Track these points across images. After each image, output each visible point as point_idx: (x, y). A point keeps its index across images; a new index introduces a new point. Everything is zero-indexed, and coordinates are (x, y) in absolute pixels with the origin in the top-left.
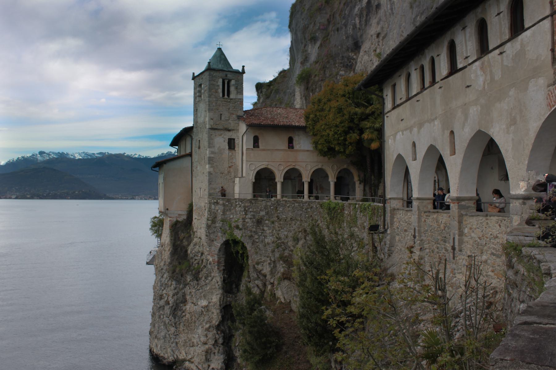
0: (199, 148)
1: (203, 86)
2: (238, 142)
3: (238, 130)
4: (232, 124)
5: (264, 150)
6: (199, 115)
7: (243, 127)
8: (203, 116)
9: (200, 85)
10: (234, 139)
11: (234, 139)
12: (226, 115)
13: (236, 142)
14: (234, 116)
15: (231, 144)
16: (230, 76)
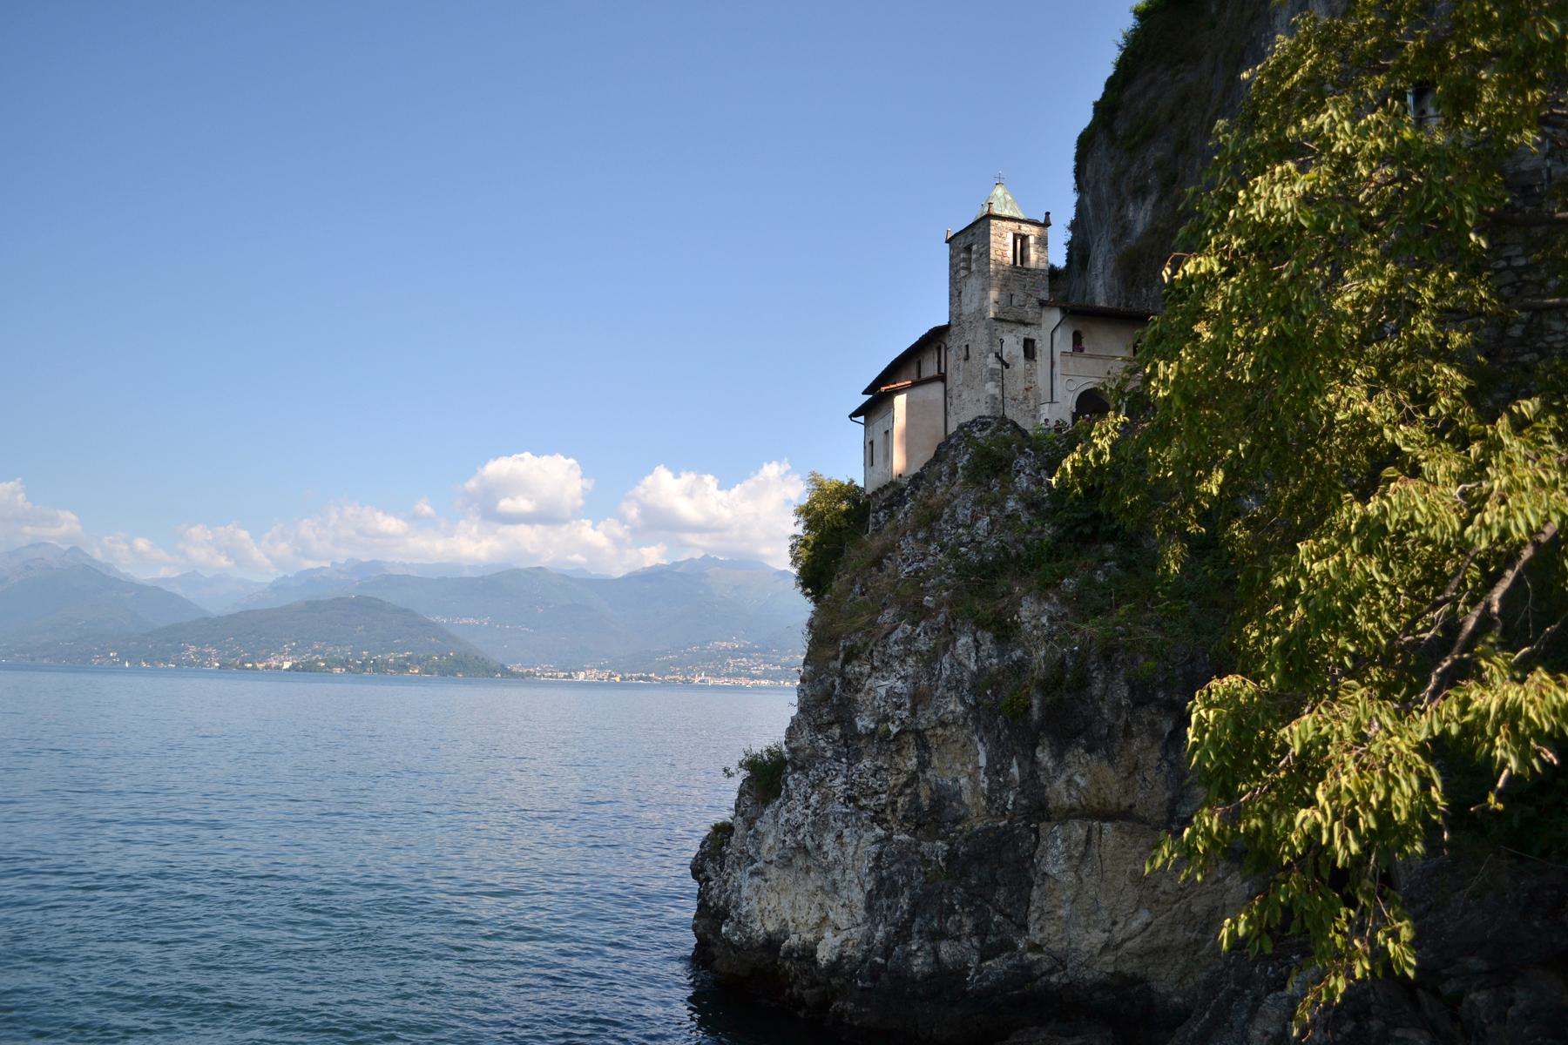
0: (967, 358)
1: (974, 248)
2: (1042, 346)
3: (1039, 325)
4: (1030, 315)
5: (1091, 356)
6: (965, 300)
7: (1054, 316)
8: (976, 300)
9: (968, 249)
10: (1033, 341)
11: (1033, 341)
12: (1019, 297)
13: (1038, 345)
14: (1033, 300)
15: (1029, 348)
16: (1025, 229)
